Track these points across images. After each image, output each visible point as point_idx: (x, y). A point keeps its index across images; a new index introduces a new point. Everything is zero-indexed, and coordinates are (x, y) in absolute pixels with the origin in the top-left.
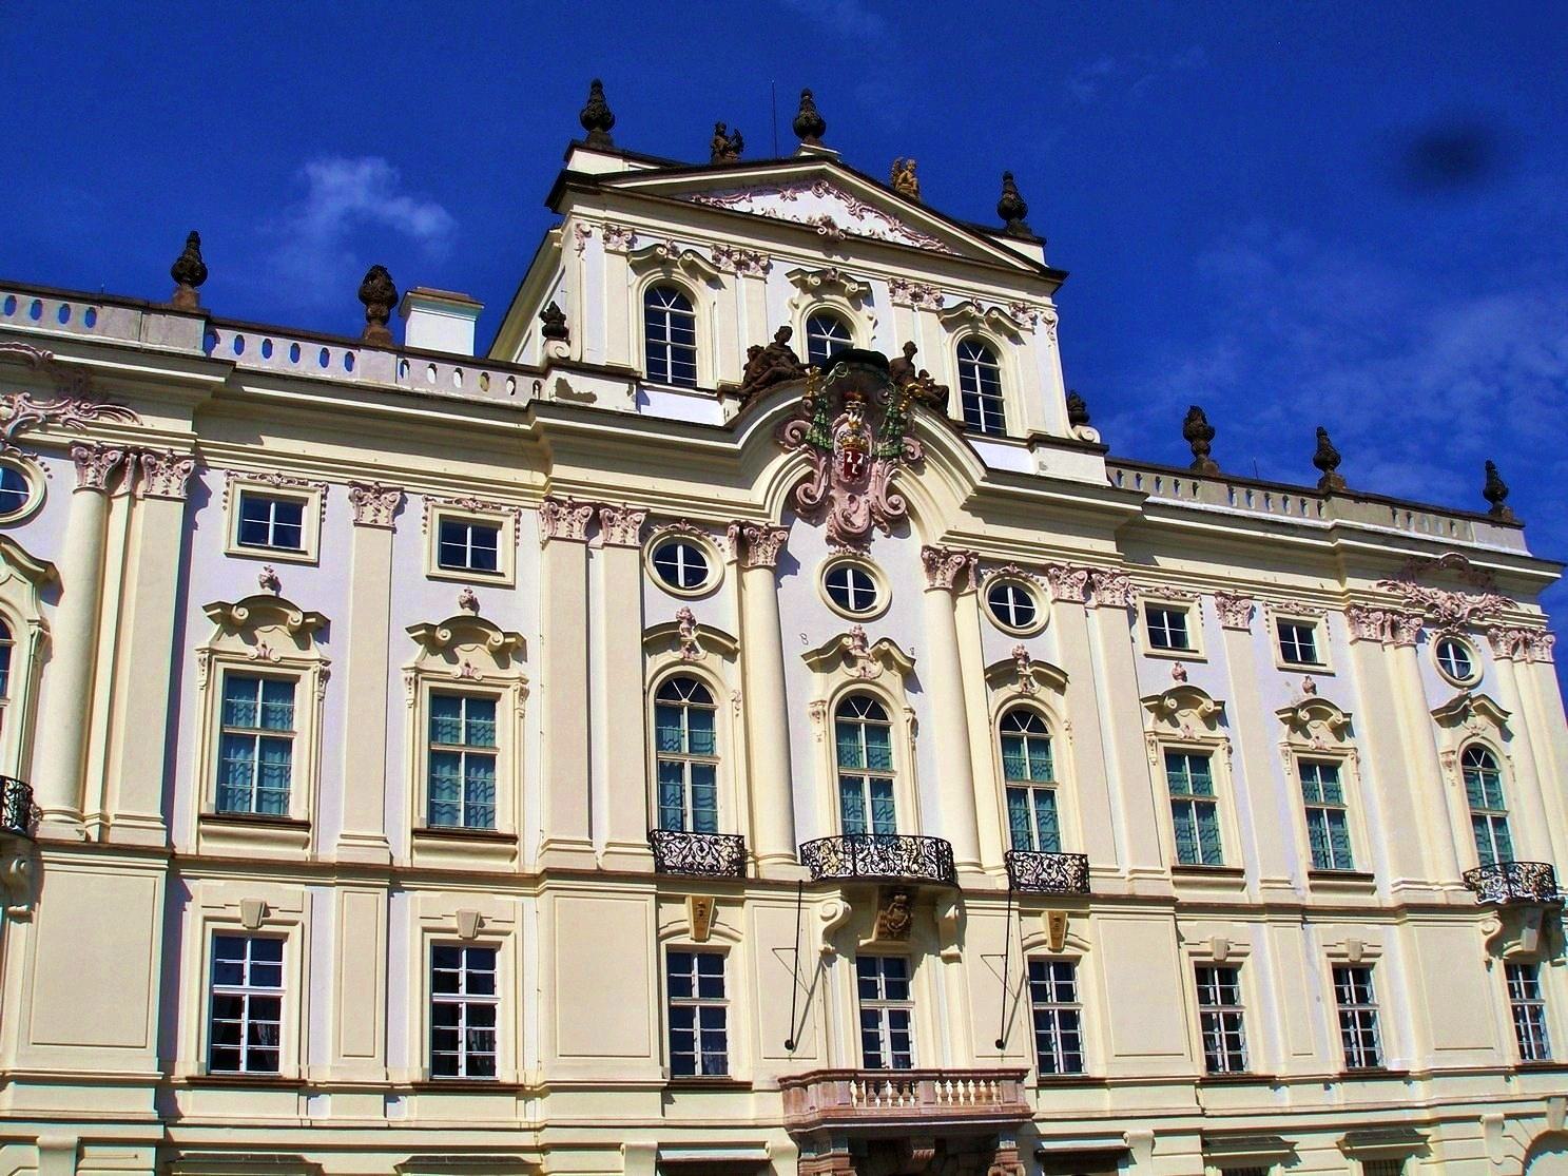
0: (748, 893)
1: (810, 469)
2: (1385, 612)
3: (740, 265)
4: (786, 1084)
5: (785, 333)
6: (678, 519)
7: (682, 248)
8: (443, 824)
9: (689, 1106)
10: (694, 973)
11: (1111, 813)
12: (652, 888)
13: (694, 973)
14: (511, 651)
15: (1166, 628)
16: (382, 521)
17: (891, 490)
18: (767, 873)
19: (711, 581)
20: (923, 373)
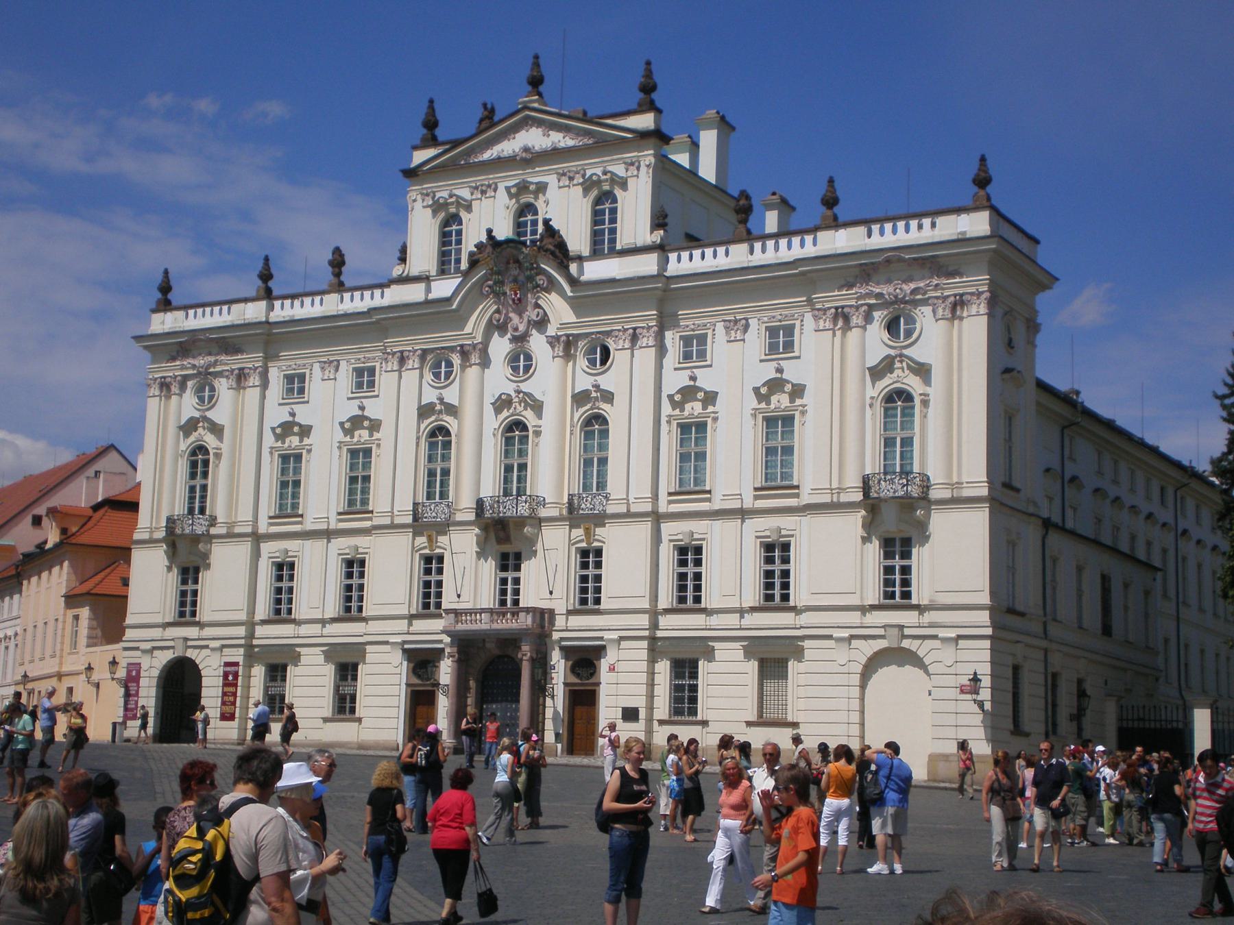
2: (836, 308)
3: (483, 192)
5: (489, 232)
7: (457, 192)
8: (353, 509)
9: (419, 625)
10: (432, 563)
11: (636, 464)
13: (432, 563)
14: (375, 426)
15: (695, 349)
17: (537, 306)
18: (459, 517)
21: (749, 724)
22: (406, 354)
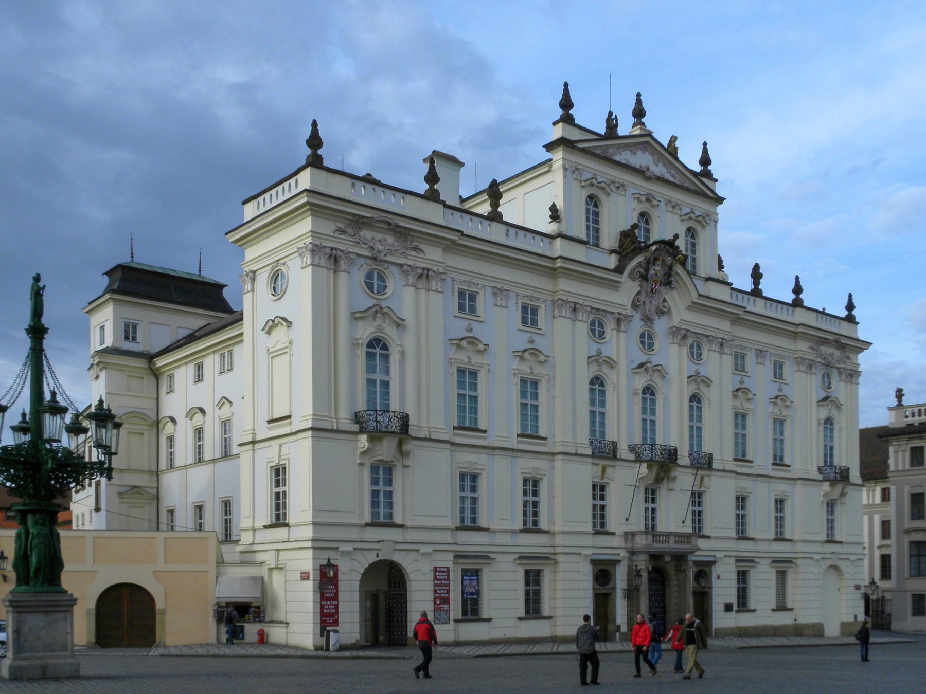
0: (618, 463)
1: (638, 289)
4: (626, 534)
5: (635, 226)
6: (598, 310)
10: (599, 491)
12: (590, 460)
13: (599, 491)
16: (504, 304)
17: (665, 300)
19: (607, 335)
20: (678, 247)
21: (773, 610)
22: (578, 306)
